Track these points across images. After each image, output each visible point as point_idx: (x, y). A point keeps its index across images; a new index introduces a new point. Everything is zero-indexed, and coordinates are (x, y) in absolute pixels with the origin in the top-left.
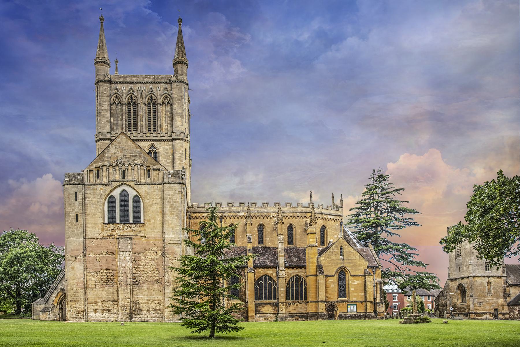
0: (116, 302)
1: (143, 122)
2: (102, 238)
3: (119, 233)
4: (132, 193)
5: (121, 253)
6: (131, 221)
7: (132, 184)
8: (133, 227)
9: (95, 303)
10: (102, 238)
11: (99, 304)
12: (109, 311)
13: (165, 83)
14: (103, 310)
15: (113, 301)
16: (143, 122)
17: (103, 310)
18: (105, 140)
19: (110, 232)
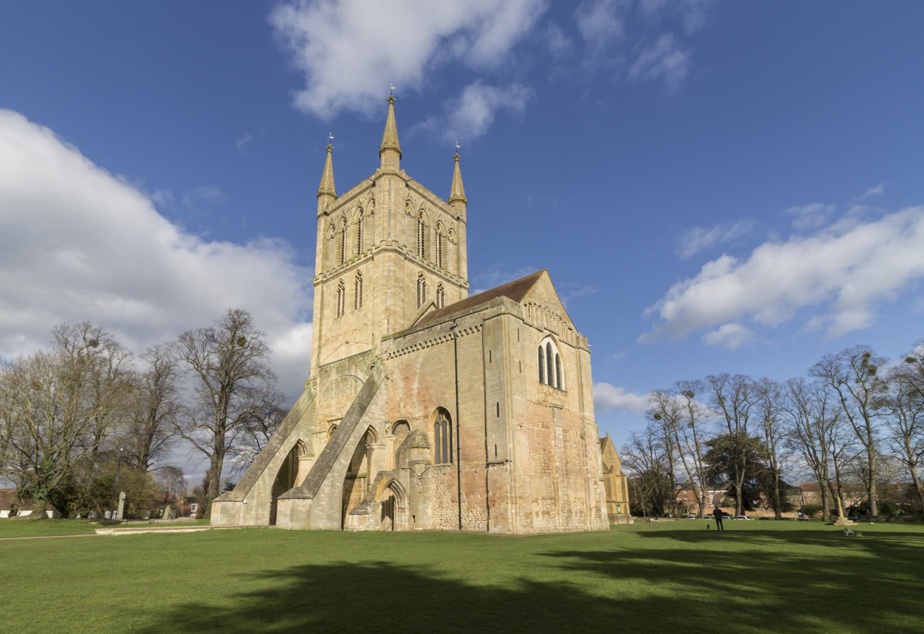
0: (554, 499)
1: (433, 252)
2: (539, 403)
3: (550, 400)
4: (555, 351)
5: (557, 428)
6: (556, 386)
7: (556, 337)
8: (560, 395)
9: (536, 501)
10: (539, 403)
11: (540, 502)
12: (548, 513)
13: (453, 217)
14: (544, 513)
15: (551, 499)
16: (433, 252)
17: (544, 513)
18: (400, 253)
19: (543, 395)
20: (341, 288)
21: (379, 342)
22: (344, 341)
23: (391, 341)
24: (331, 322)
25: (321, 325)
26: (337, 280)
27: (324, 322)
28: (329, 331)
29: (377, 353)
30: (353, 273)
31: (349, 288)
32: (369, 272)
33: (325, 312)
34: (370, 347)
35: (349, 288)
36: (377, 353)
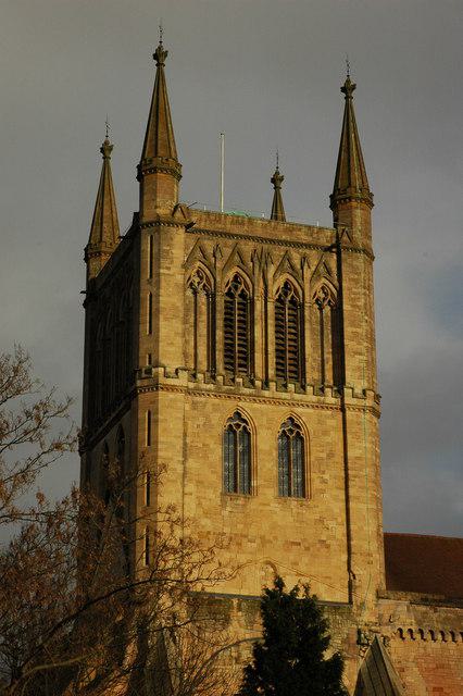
20: (238, 435)
21: (371, 597)
22: (261, 558)
23: (403, 607)
24: (213, 496)
25: (184, 494)
26: (230, 406)
27: (191, 487)
28: (206, 514)
29: (367, 617)
30: (280, 414)
31: (266, 443)
32: (325, 433)
33: (191, 463)
34: (341, 596)
35: (266, 443)
36: (367, 617)
